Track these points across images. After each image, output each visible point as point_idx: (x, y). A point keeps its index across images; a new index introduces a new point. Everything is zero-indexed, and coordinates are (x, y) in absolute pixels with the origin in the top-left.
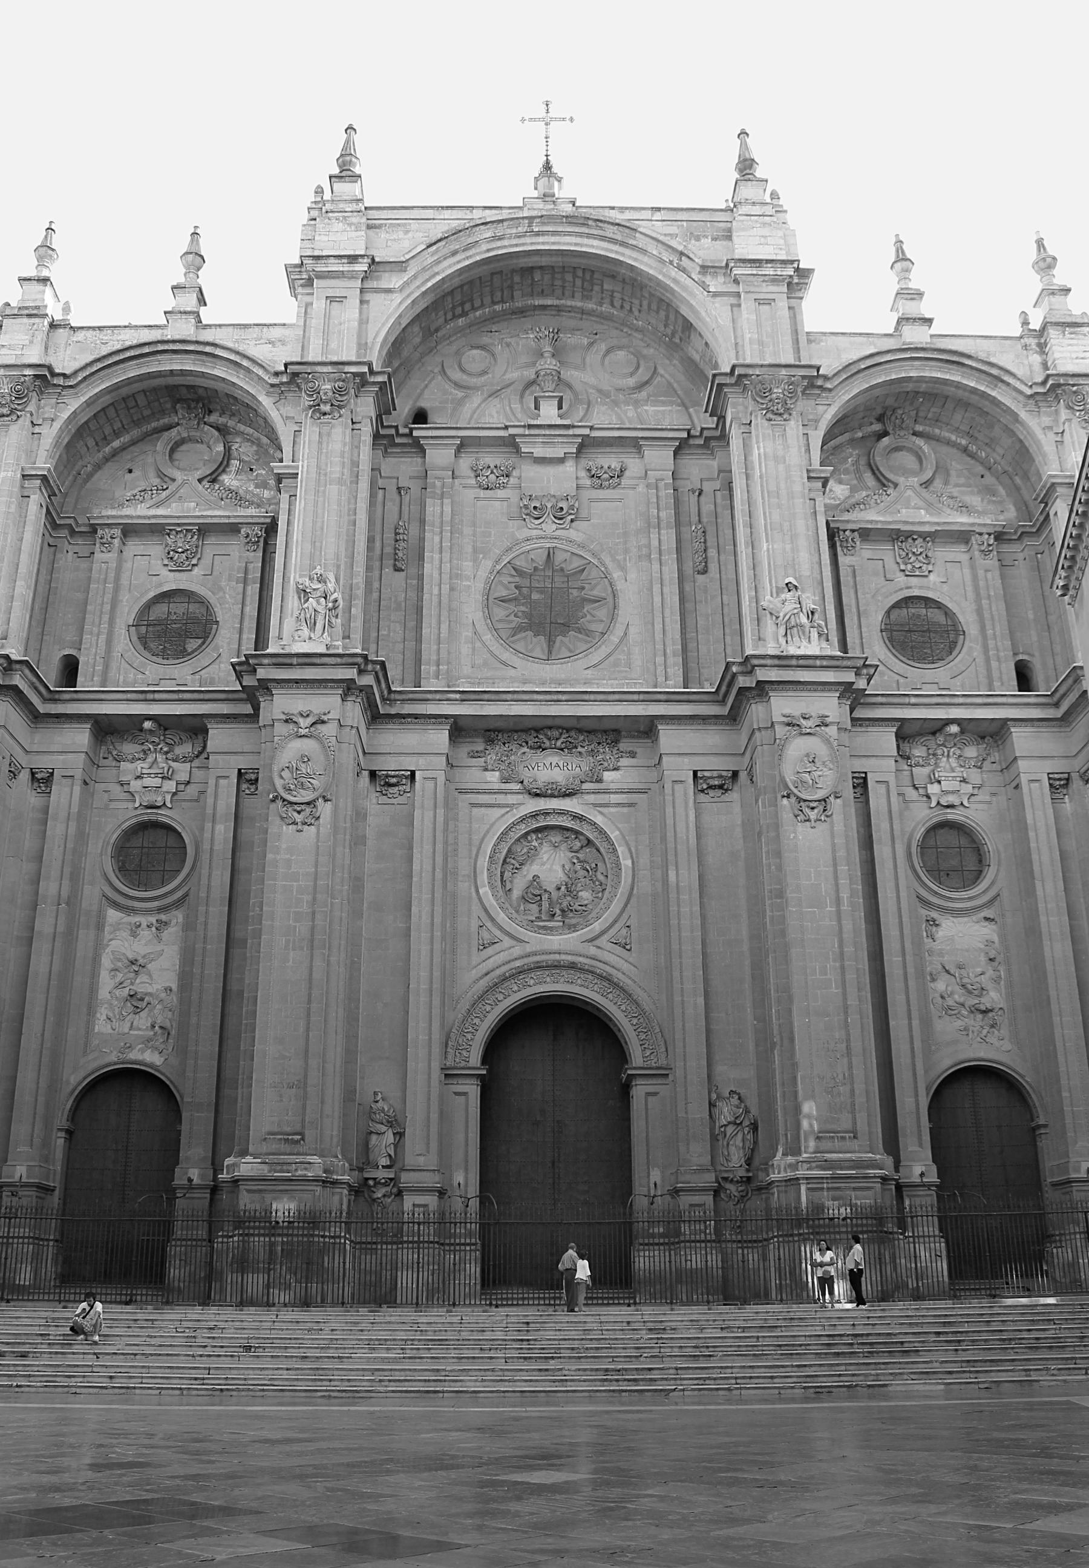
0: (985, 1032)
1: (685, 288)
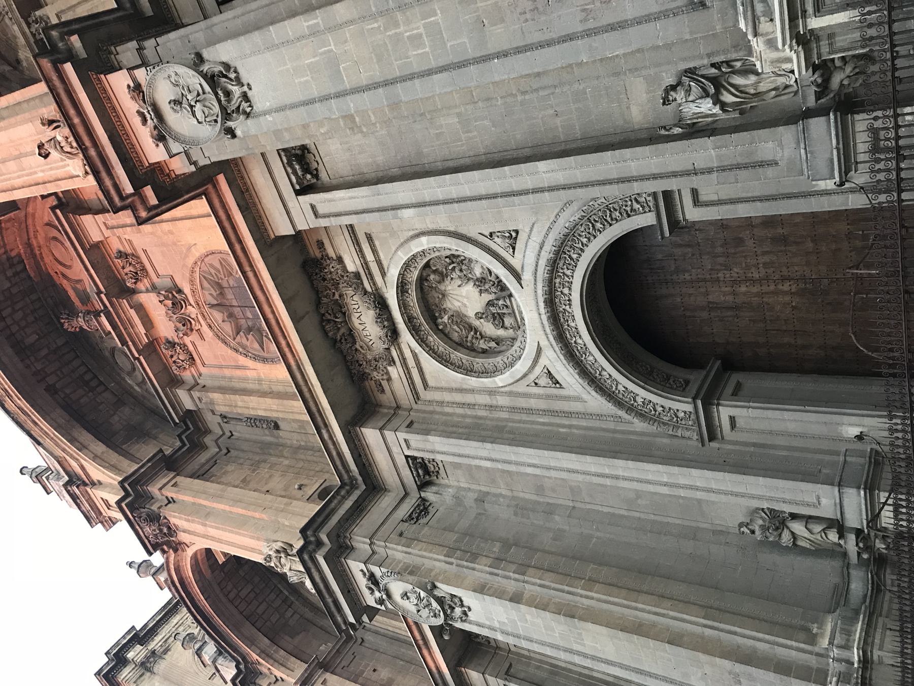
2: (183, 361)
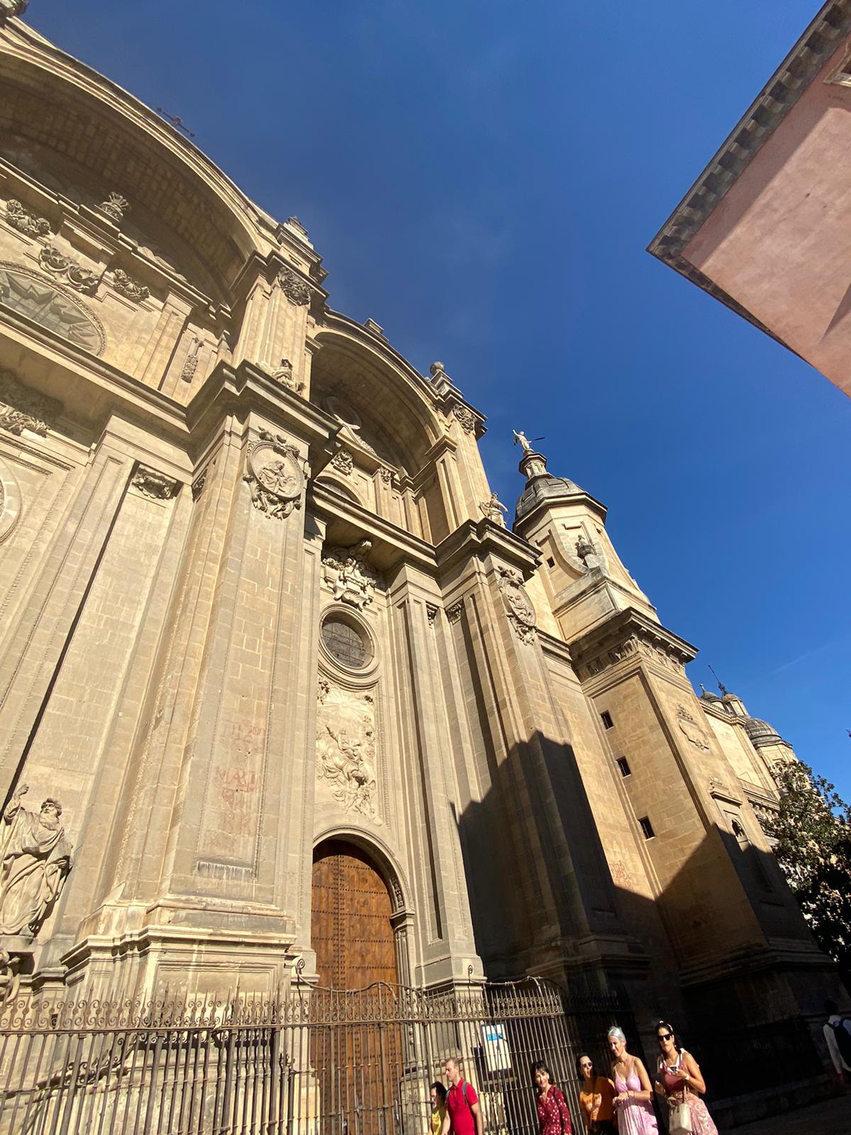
0: (359, 801)
1: (245, 223)
2: (20, 218)
